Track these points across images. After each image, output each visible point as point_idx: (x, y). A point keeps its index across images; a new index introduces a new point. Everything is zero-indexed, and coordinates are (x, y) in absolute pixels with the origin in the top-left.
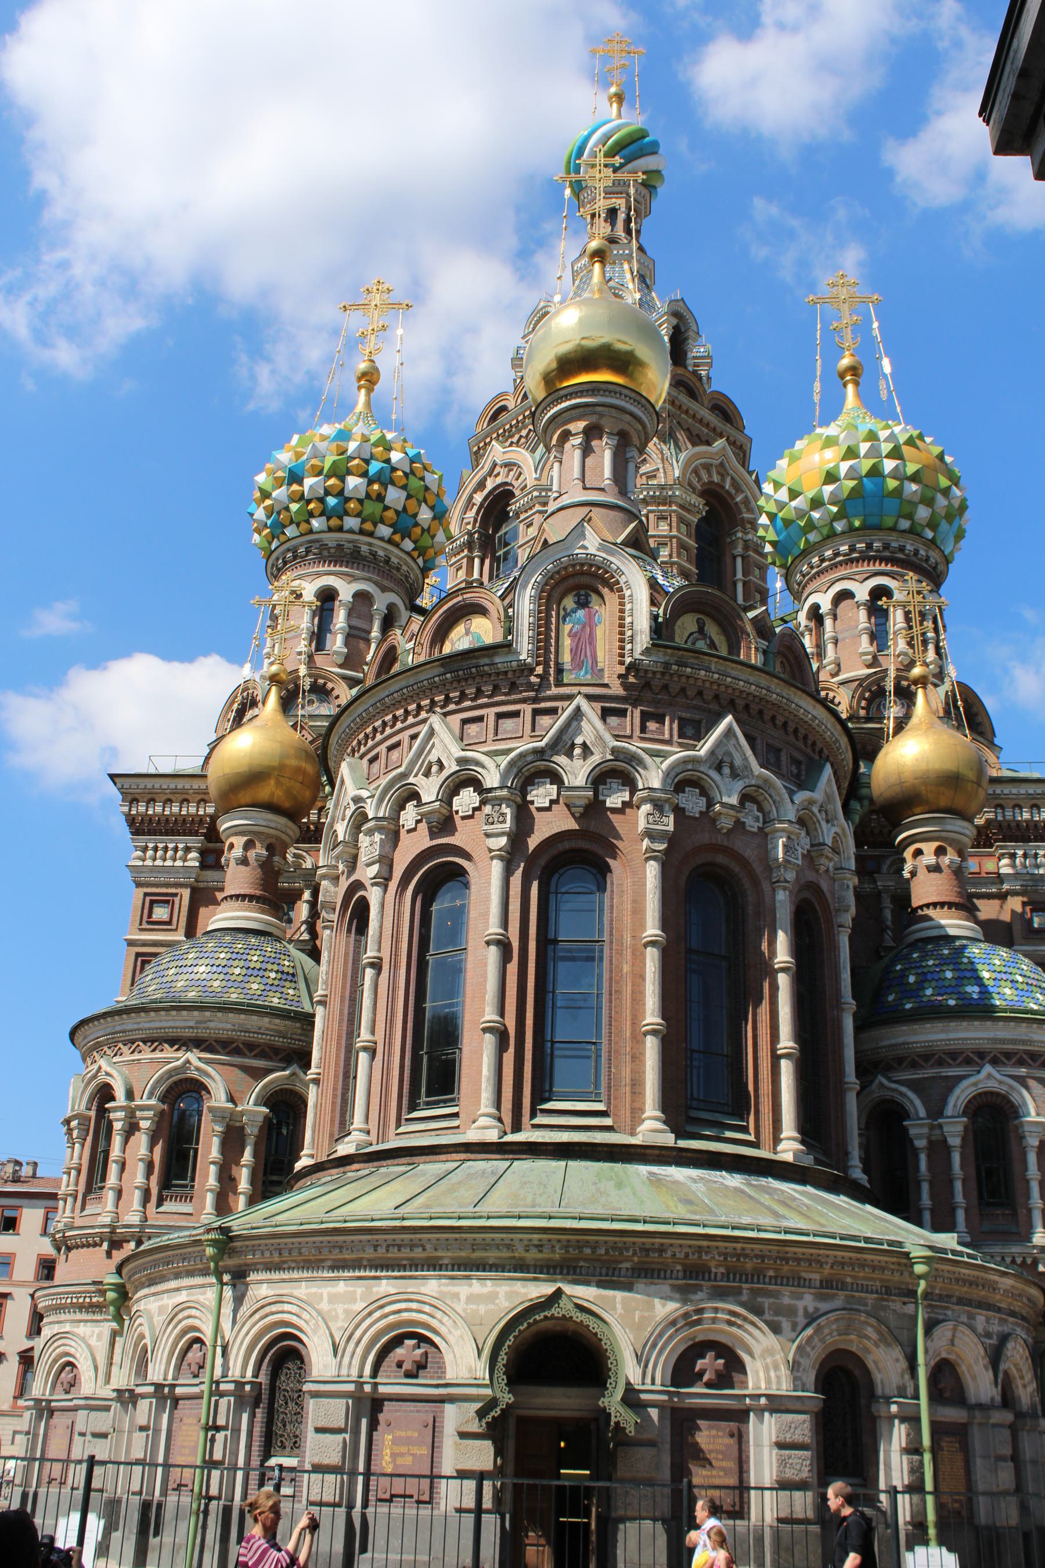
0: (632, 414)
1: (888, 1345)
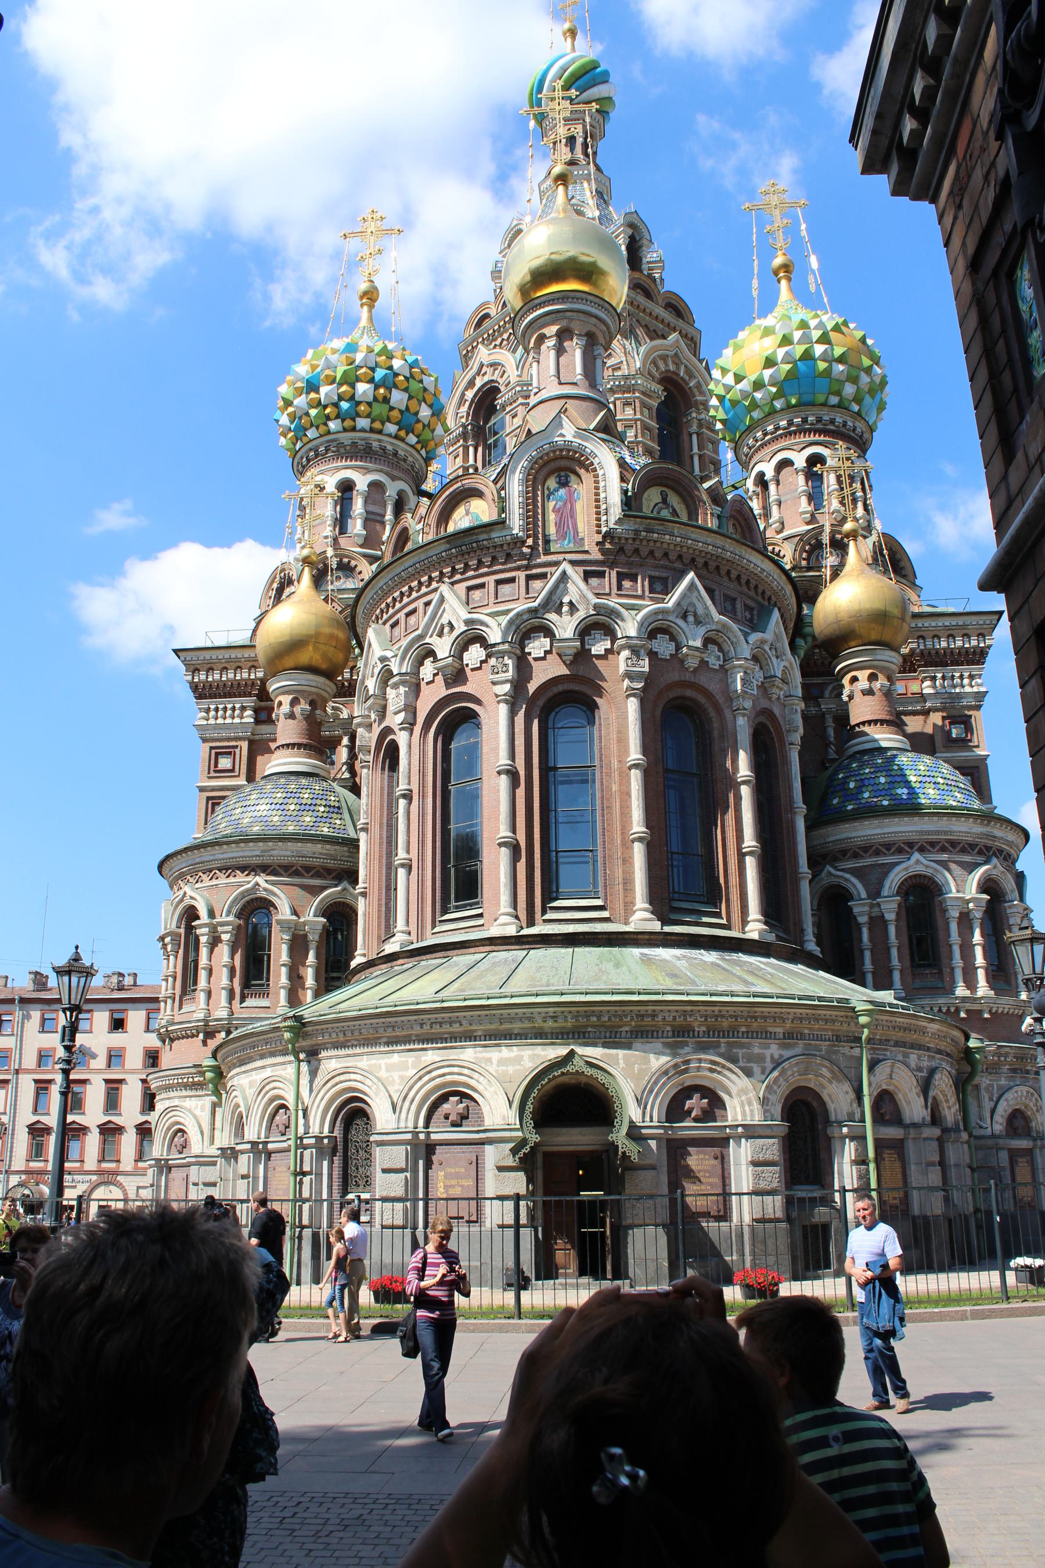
1: (839, 1081)
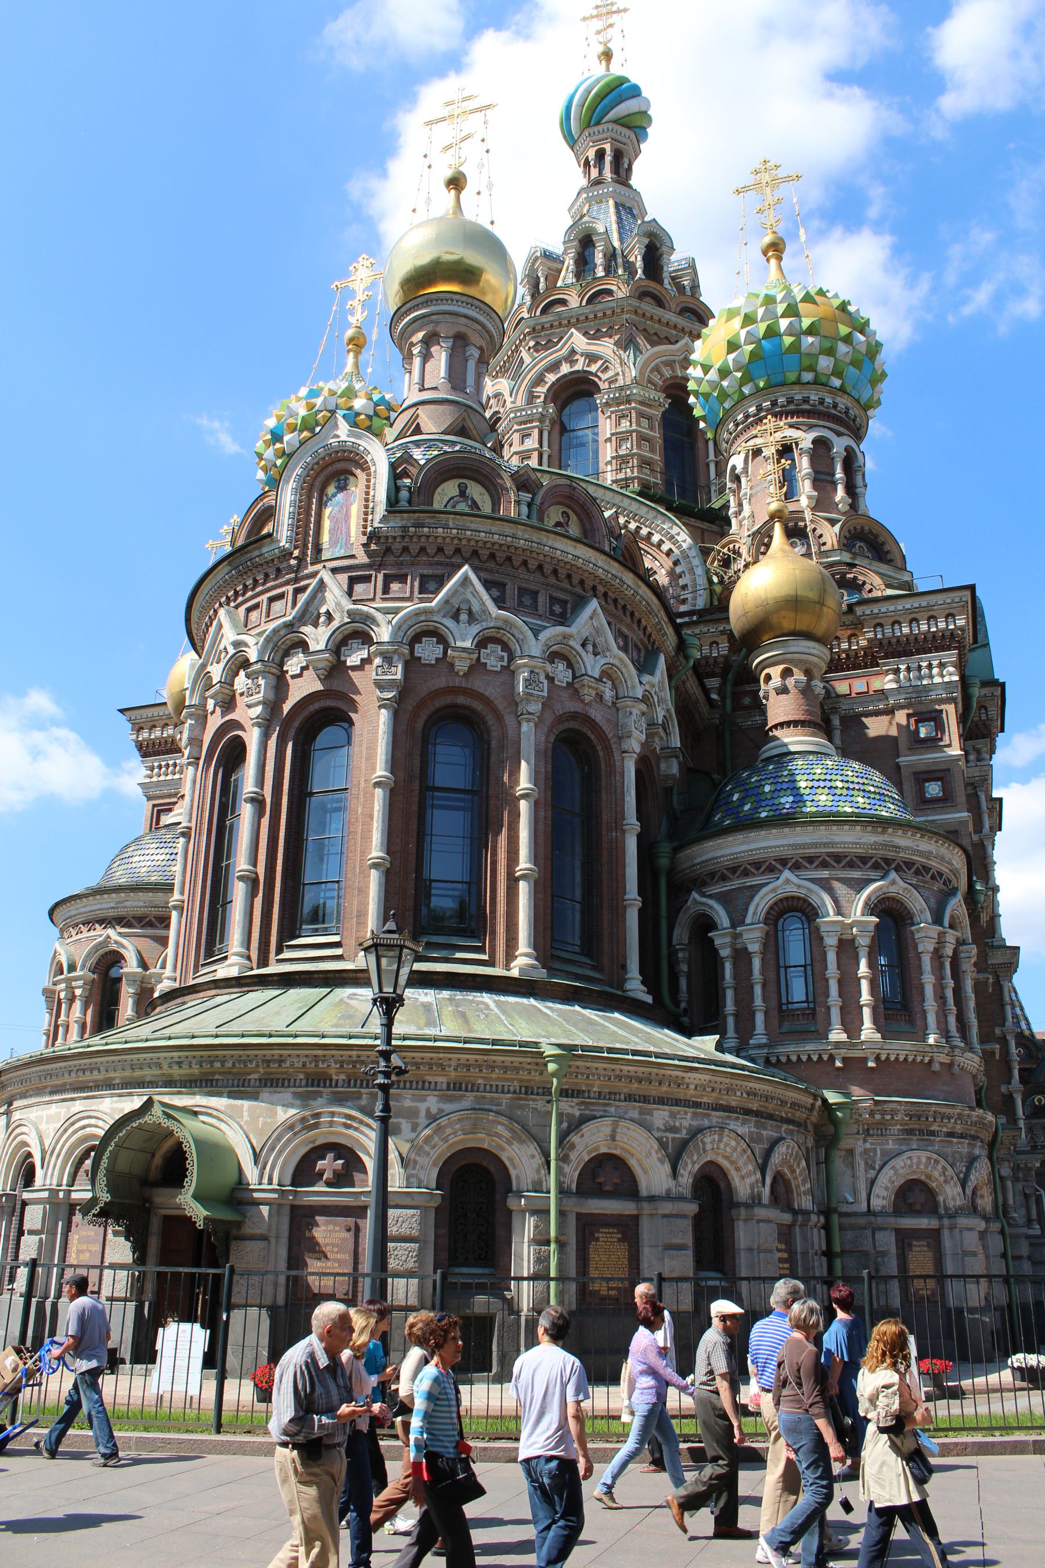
0: (466, 317)
1: (521, 1142)
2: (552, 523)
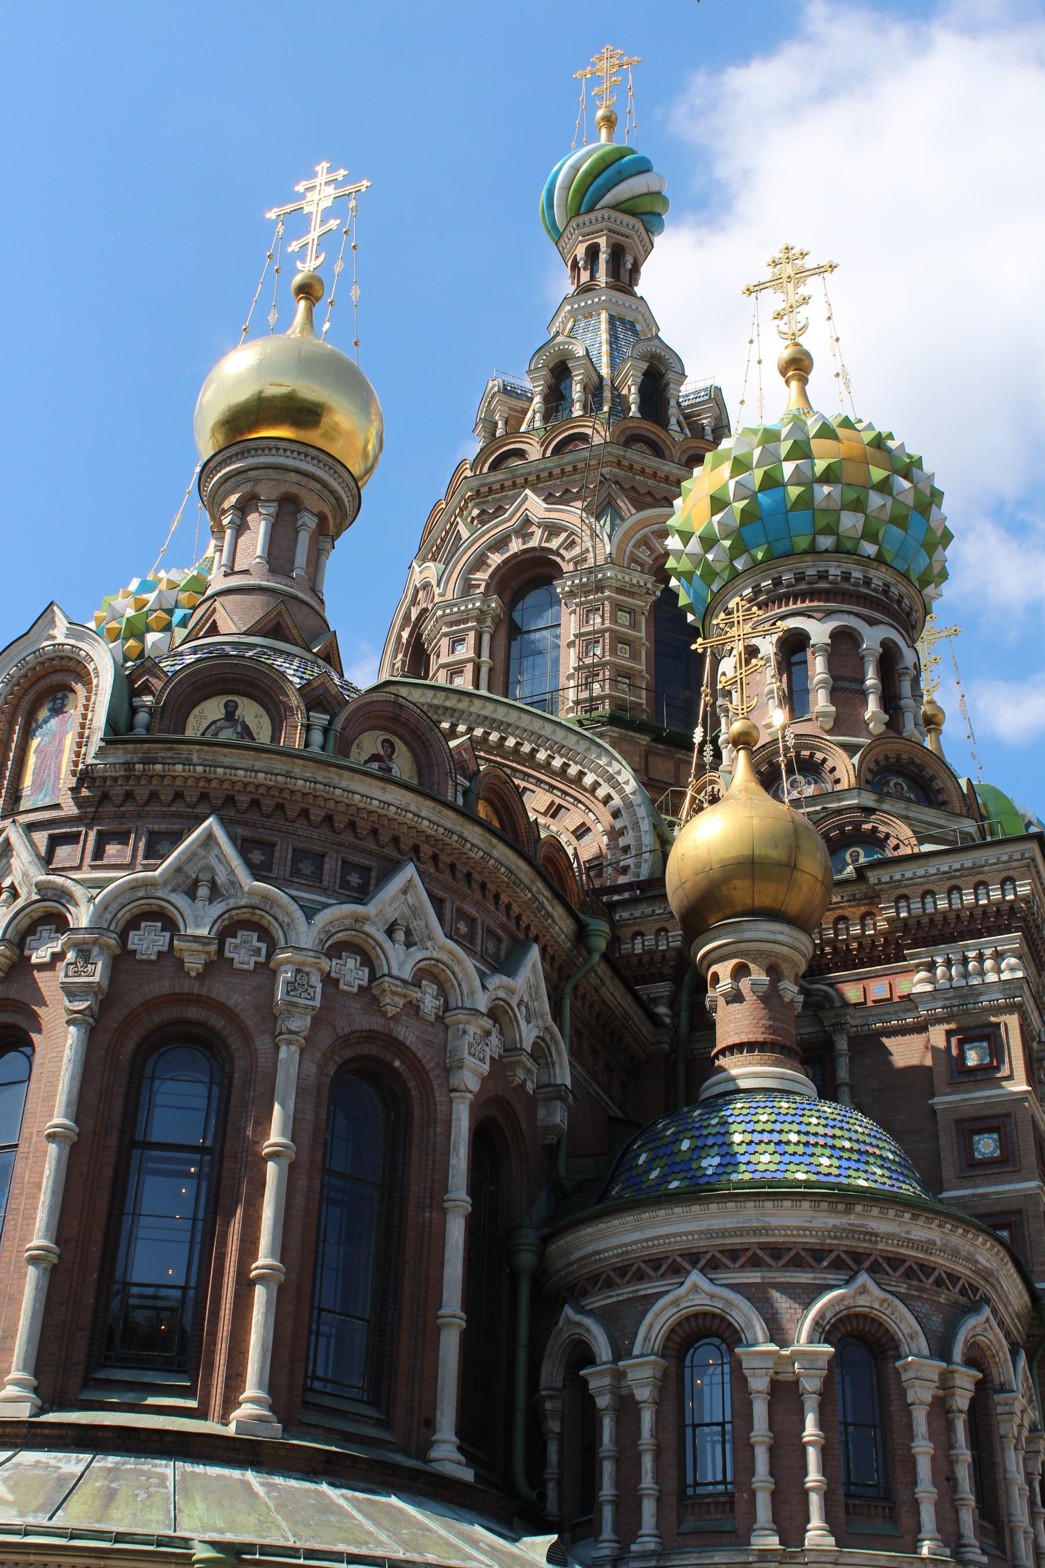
2: (365, 756)
